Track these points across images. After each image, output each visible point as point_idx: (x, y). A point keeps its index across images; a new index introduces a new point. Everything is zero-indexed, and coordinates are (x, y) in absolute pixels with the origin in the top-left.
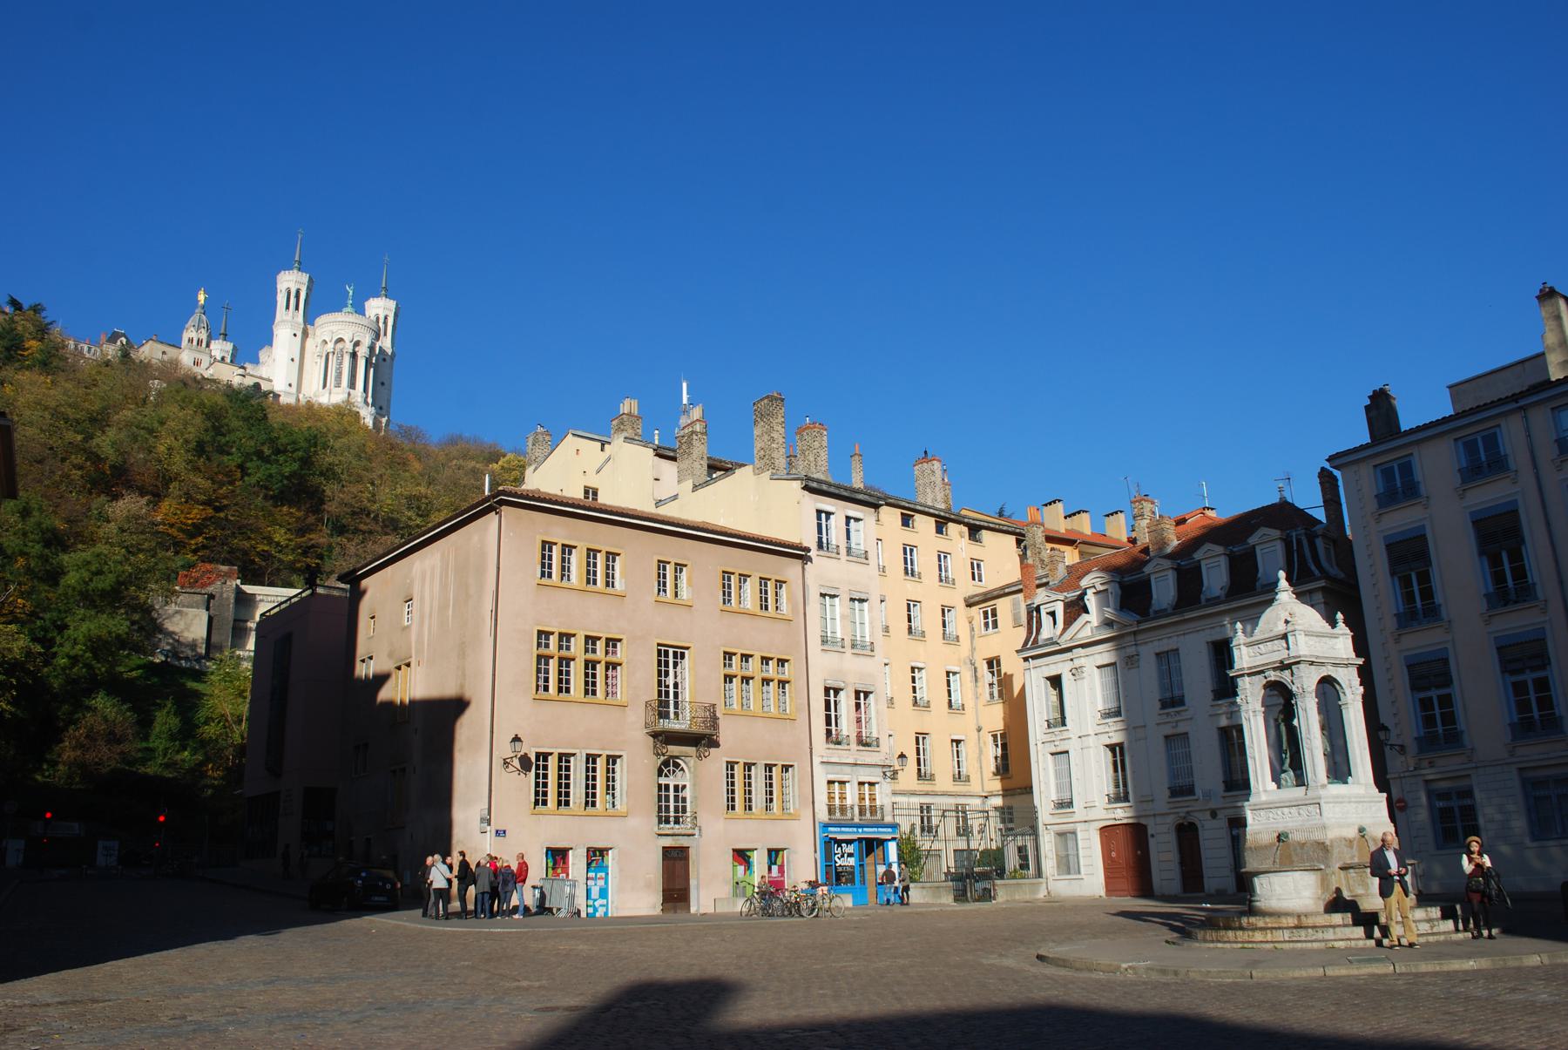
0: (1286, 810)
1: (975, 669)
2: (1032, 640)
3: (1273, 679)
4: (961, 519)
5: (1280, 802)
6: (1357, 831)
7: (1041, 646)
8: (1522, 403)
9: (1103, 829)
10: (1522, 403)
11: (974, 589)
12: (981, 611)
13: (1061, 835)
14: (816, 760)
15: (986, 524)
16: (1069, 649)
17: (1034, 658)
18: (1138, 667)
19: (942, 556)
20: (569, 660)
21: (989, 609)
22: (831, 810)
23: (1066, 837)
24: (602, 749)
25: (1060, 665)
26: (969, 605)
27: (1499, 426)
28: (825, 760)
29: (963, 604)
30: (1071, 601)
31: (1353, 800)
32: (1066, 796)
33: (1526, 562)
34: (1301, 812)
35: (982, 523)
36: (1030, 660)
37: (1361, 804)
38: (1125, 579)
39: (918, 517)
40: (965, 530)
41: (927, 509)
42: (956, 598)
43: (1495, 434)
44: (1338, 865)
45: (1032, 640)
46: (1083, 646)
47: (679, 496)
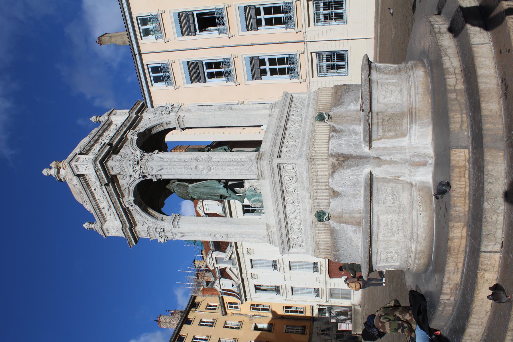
0: (289, 208)
1: (255, 315)
2: (237, 295)
3: (132, 198)
4: (186, 311)
5: (279, 214)
6: (322, 123)
7: (240, 292)
8: (136, 52)
9: (330, 277)
10: (136, 52)
11: (220, 310)
12: (229, 309)
13: (331, 296)
15: (192, 299)
16: (243, 280)
17: (245, 296)
18: (253, 249)
19: (201, 323)
21: (228, 305)
23: (332, 294)
25: (250, 285)
26: (226, 314)
27: (147, 65)
29: (225, 316)
30: (221, 274)
31: (283, 124)
32: (313, 291)
33: (213, 61)
34: (290, 190)
35: (191, 301)
36: (246, 298)
37: (291, 117)
38: (212, 248)
39: (181, 333)
40: (193, 309)
41: (178, 328)
42: (221, 319)
43: (151, 67)
44: (366, 149)
45: (237, 295)
46: (241, 273)
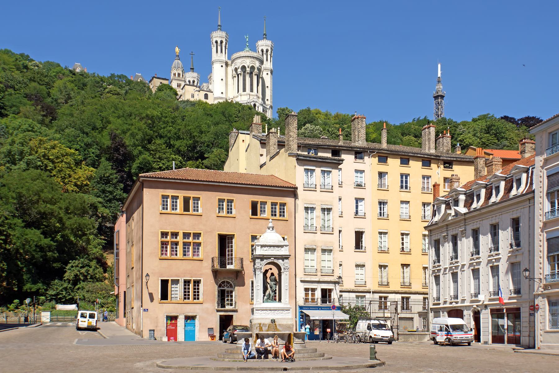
14: (298, 280)
20: (177, 244)
22: (306, 300)
24: (191, 277)
28: (303, 279)
47: (266, 163)
